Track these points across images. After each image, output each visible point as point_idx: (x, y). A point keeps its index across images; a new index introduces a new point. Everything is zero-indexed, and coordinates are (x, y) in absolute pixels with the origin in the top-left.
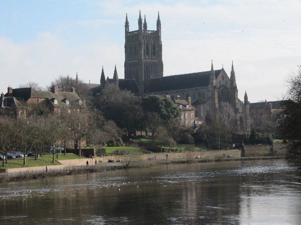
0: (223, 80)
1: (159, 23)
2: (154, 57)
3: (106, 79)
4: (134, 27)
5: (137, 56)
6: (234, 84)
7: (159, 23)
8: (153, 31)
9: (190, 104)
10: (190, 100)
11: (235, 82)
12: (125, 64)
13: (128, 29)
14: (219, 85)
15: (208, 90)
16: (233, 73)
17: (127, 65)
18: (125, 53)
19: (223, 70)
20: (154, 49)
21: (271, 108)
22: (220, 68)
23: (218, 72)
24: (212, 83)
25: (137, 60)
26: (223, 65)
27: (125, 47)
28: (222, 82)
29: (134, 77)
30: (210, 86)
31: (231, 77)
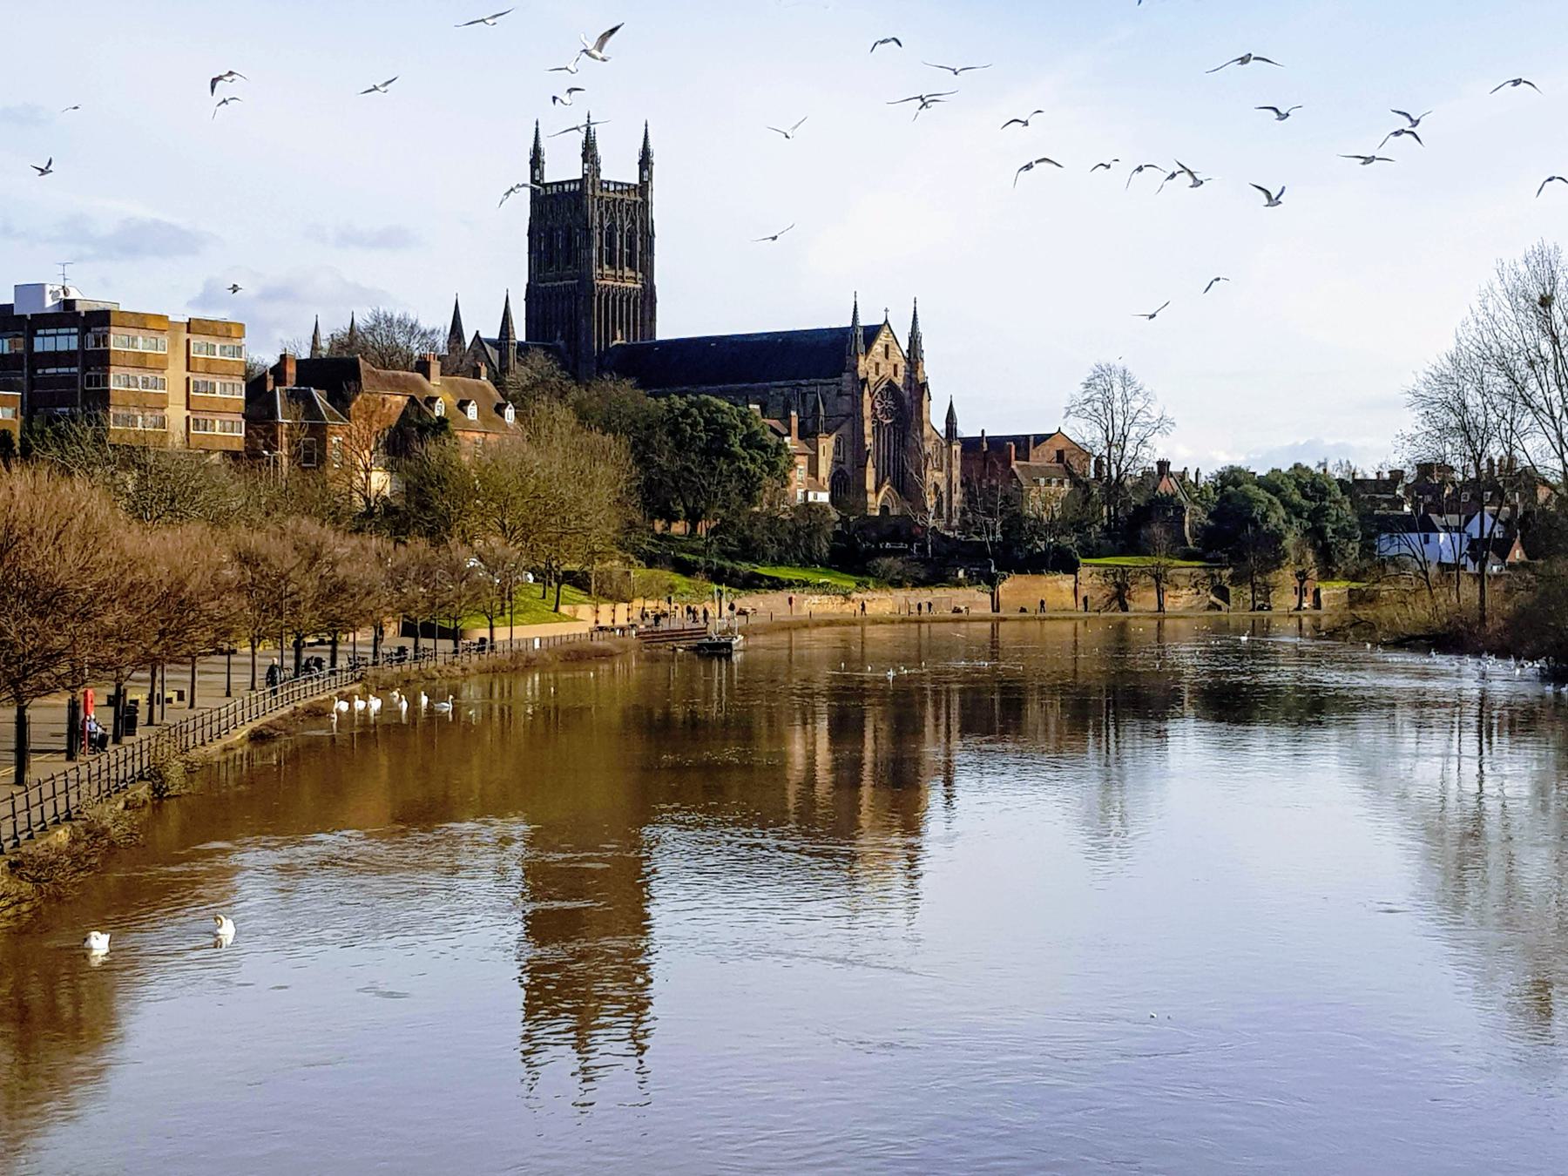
0: (887, 357)
1: (645, 162)
2: (627, 272)
3: (468, 339)
4: (563, 167)
5: (575, 266)
6: (920, 376)
7: (645, 162)
8: (629, 185)
9: (795, 432)
10: (795, 423)
11: (922, 366)
12: (527, 290)
13: (542, 173)
14: (873, 375)
15: (839, 391)
16: (914, 339)
17: (533, 296)
18: (530, 253)
19: (886, 321)
20: (631, 245)
21: (1013, 457)
22: (881, 322)
23: (872, 333)
24: (856, 367)
25: (573, 279)
26: (886, 310)
27: (530, 234)
28: (882, 366)
29: (559, 334)
30: (846, 376)
31: (908, 351)
